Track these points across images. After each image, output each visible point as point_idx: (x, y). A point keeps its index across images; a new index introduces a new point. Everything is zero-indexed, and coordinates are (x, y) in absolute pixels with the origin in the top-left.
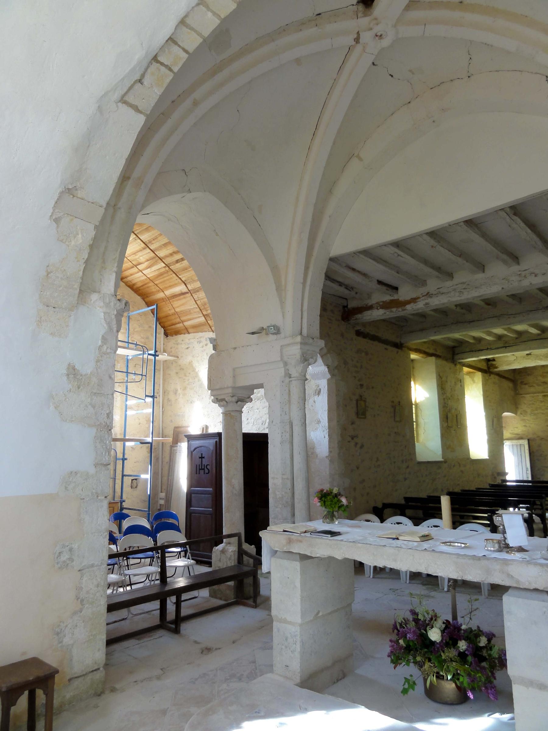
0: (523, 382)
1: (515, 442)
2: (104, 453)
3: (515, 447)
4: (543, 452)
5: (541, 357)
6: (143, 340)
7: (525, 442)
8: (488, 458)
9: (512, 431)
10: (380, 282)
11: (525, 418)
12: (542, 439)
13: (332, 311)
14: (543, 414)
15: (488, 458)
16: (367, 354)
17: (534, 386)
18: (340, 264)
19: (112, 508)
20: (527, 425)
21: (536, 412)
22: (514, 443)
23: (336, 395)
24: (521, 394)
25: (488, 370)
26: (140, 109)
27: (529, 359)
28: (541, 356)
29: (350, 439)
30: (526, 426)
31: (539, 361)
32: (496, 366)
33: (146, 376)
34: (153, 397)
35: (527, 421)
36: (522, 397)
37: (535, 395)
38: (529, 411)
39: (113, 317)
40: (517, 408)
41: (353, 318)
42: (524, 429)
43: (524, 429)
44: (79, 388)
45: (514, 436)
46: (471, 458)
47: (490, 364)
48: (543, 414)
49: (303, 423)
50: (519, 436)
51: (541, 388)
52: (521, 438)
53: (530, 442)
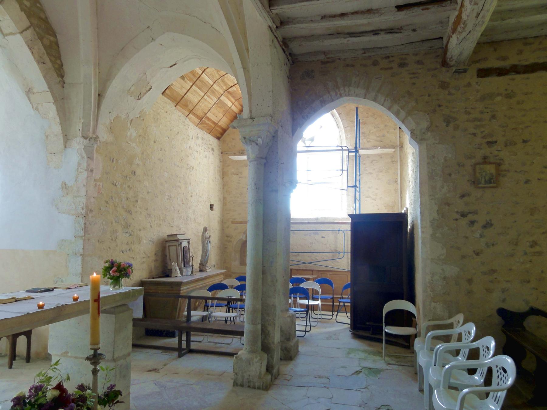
2: (80, 230)
6: (379, 139)
10: (400, 8)
13: (419, 62)
16: (509, 96)
18: (311, 21)
19: (346, 276)
23: (428, 164)
26: (14, 32)
29: (458, 216)
33: (347, 170)
34: (355, 186)
39: (82, 149)
41: (448, 59)
44: (67, 194)
49: (253, 203)
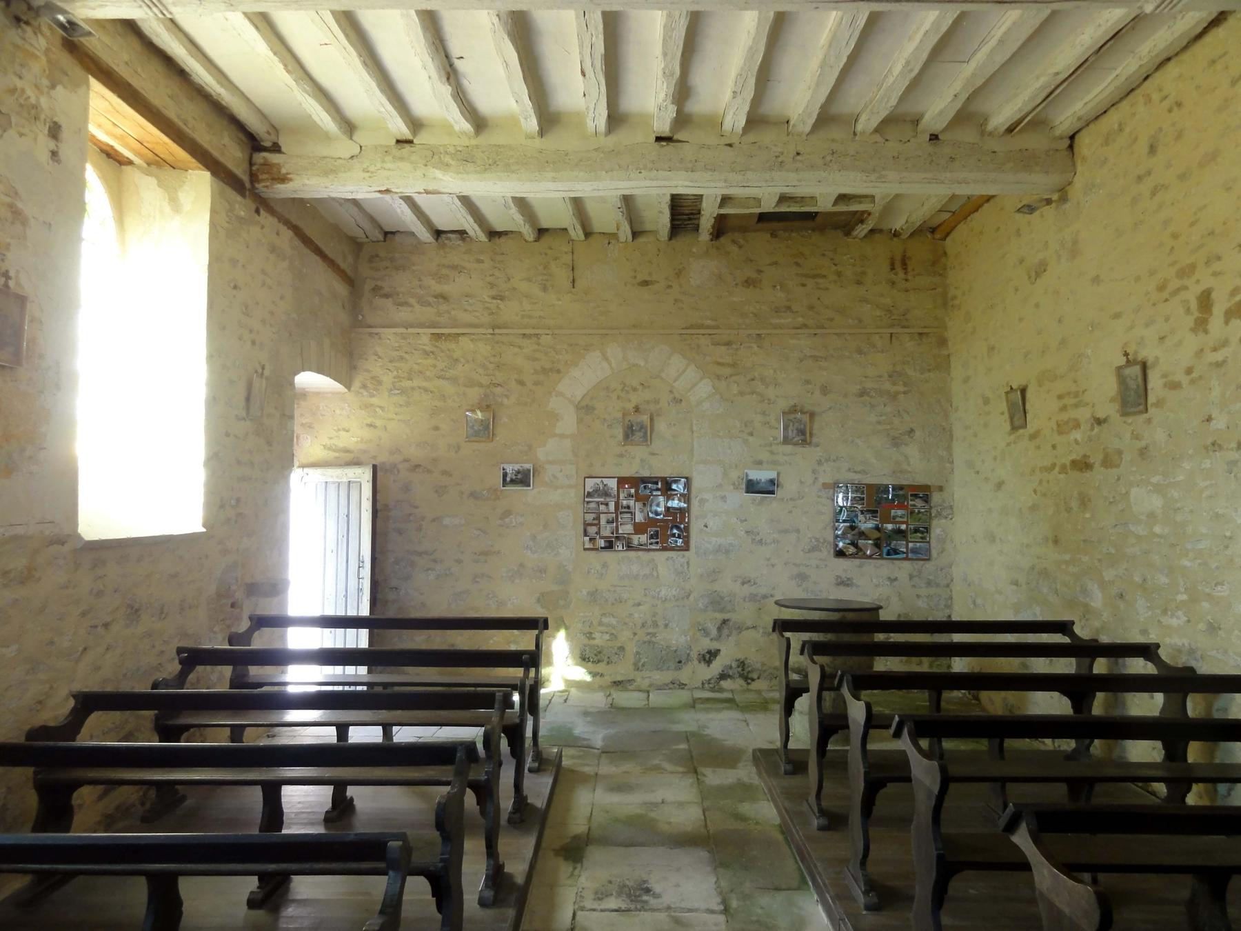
0: (381, 288)
1: (334, 474)
3: (332, 490)
4: (416, 507)
5: (447, 159)
7: (364, 476)
8: (204, 530)
9: (331, 438)
11: (374, 400)
12: (418, 466)
14: (426, 390)
15: (204, 530)
17: (411, 306)
20: (379, 423)
21: (407, 384)
22: (332, 477)
24: (370, 327)
25: (248, 185)
27: (402, 159)
28: (446, 153)
30: (375, 427)
31: (438, 174)
32: (284, 171)
35: (378, 410)
36: (371, 334)
37: (410, 330)
38: (387, 379)
40: (353, 367)
42: (367, 434)
43: (367, 434)
45: (337, 454)
46: (79, 537)
47: (262, 161)
48: (426, 390)
50: (348, 457)
51: (428, 313)
52: (356, 463)
53: (380, 474)
